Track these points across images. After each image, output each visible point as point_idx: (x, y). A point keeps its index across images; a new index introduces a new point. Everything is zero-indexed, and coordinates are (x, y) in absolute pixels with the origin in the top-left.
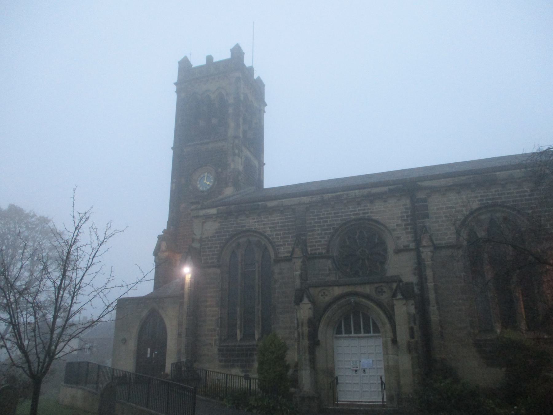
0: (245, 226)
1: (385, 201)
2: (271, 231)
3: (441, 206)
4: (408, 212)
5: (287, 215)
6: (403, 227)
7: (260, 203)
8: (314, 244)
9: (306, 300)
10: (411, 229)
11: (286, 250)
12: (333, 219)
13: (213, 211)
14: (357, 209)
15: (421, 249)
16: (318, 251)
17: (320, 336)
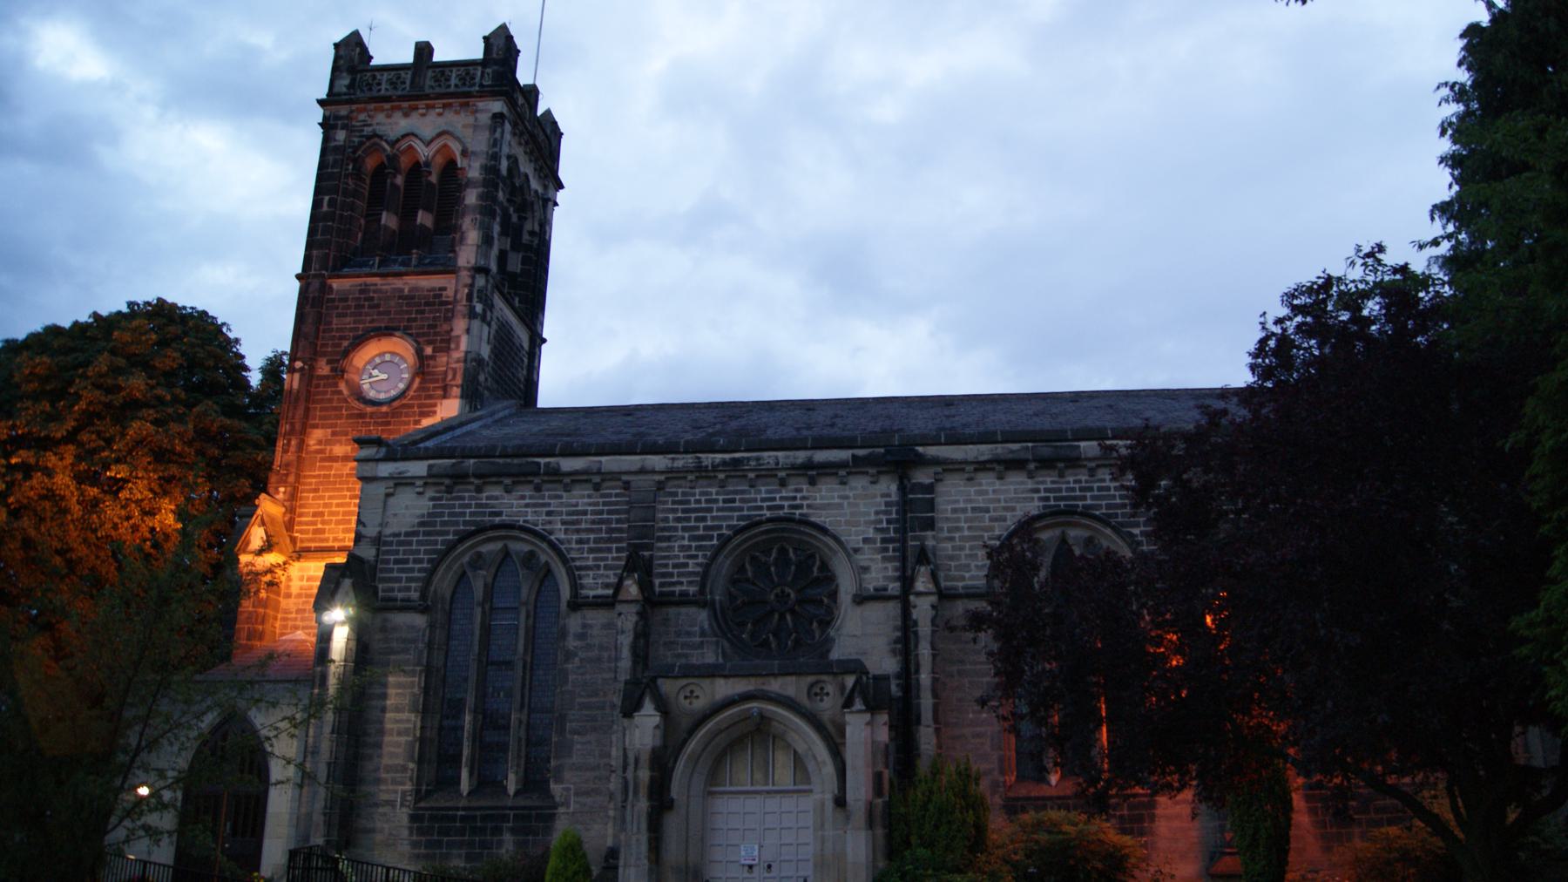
0: (499, 514)
1: (843, 483)
2: (566, 530)
3: (962, 505)
4: (889, 513)
5: (610, 495)
6: (879, 545)
7: (542, 461)
8: (671, 570)
9: (648, 707)
10: (894, 550)
11: (600, 582)
12: (720, 514)
13: (418, 468)
14: (778, 496)
15: (912, 598)
16: (677, 589)
17: (676, 790)
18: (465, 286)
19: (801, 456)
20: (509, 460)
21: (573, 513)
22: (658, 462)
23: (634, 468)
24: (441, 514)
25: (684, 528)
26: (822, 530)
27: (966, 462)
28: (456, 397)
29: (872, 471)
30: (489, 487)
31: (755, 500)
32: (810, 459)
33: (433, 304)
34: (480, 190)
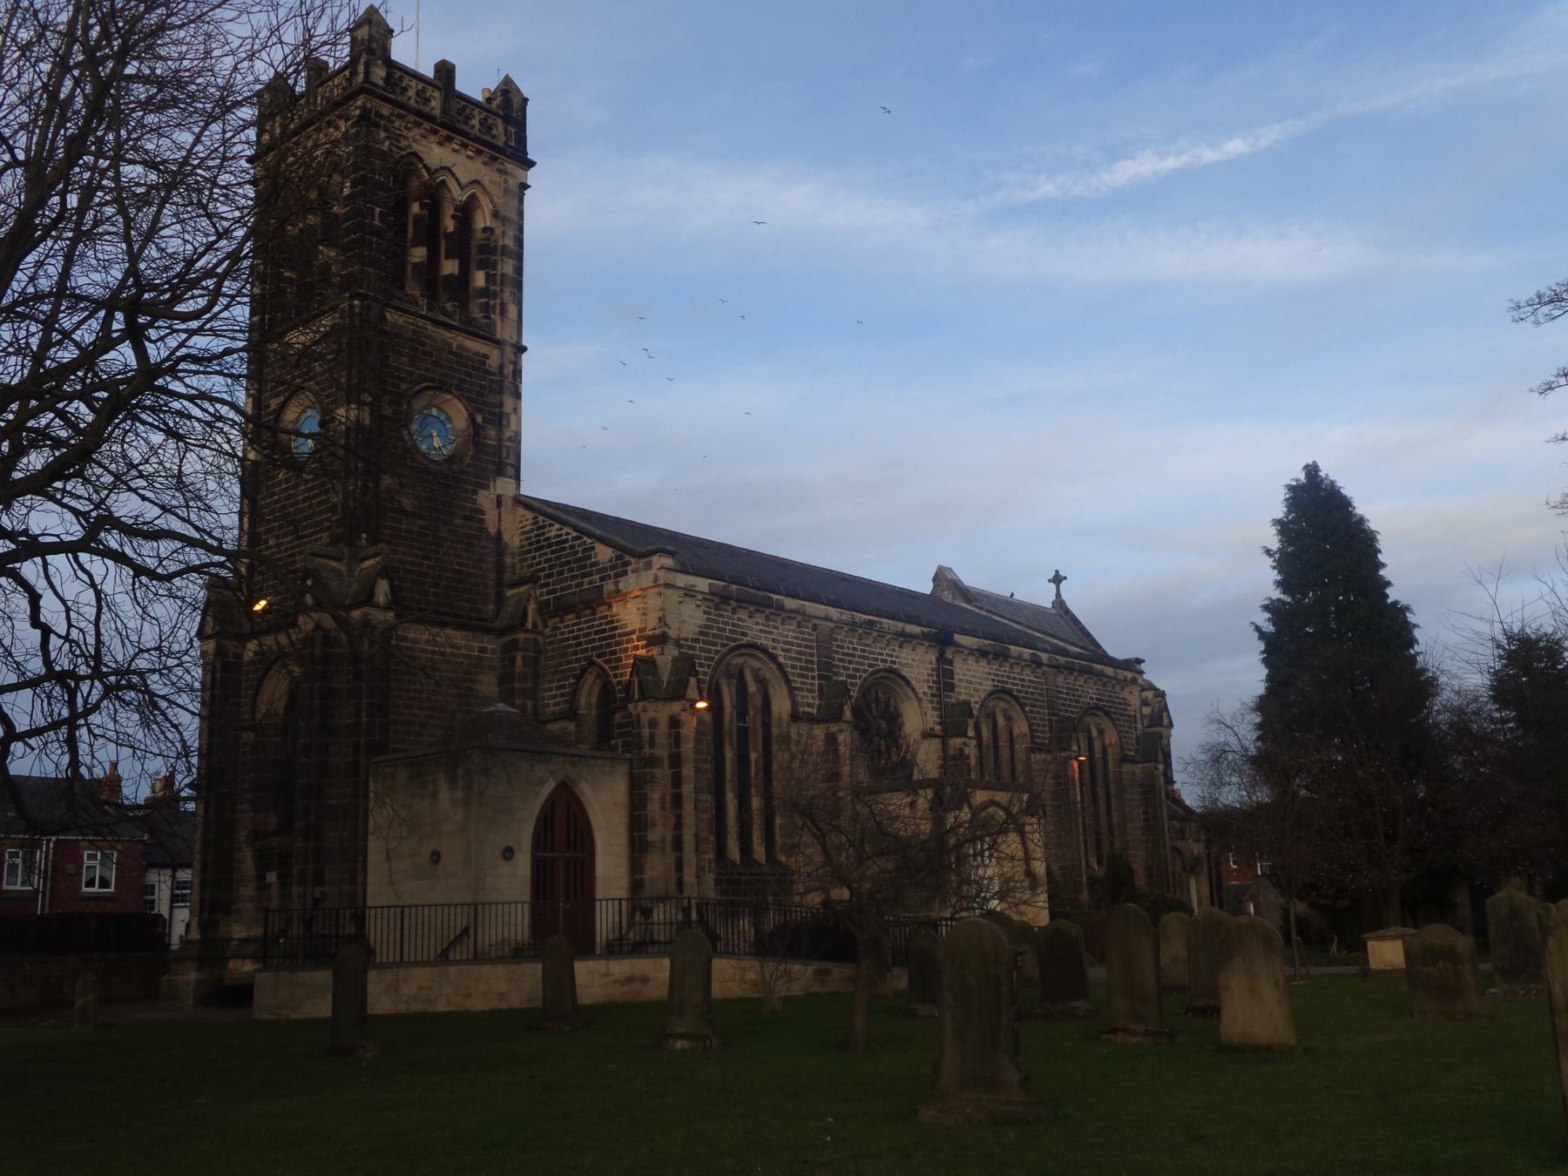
0: (745, 634)
5: (803, 633)
7: (775, 597)
13: (703, 584)
18: (511, 362)
19: (900, 625)
20: (755, 591)
21: (786, 643)
22: (834, 612)
23: (823, 615)
24: (711, 628)
25: (844, 668)
26: (908, 682)
27: (966, 648)
28: (510, 477)
29: (927, 644)
30: (739, 611)
31: (874, 653)
32: (903, 629)
33: (477, 369)
34: (516, 262)
